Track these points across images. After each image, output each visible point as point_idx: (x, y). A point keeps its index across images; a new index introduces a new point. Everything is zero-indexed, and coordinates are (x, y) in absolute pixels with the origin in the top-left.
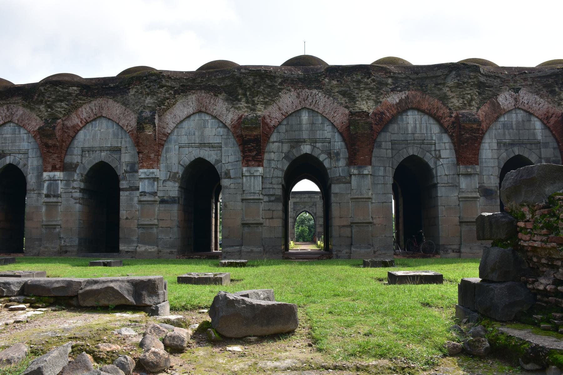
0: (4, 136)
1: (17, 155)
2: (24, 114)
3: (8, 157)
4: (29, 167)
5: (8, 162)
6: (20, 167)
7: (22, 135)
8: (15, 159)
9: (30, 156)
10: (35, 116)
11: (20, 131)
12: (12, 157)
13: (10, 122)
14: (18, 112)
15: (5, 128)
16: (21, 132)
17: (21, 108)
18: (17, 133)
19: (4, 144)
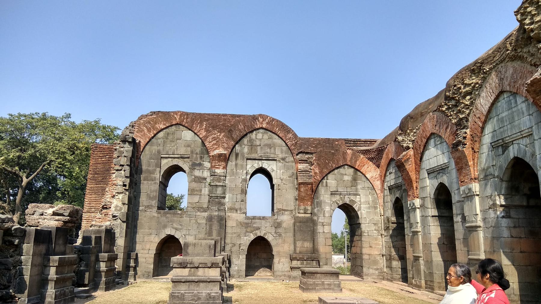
0: (500, 117)
1: (521, 141)
2: (515, 71)
3: (511, 148)
4: (538, 156)
5: (512, 156)
6: (527, 159)
7: (519, 107)
8: (519, 149)
9: (536, 138)
10: (529, 67)
11: (516, 101)
12: (516, 146)
13: (501, 92)
14: (508, 72)
15: (499, 104)
16: (519, 102)
17: (509, 64)
18: (513, 105)
19: (502, 130)
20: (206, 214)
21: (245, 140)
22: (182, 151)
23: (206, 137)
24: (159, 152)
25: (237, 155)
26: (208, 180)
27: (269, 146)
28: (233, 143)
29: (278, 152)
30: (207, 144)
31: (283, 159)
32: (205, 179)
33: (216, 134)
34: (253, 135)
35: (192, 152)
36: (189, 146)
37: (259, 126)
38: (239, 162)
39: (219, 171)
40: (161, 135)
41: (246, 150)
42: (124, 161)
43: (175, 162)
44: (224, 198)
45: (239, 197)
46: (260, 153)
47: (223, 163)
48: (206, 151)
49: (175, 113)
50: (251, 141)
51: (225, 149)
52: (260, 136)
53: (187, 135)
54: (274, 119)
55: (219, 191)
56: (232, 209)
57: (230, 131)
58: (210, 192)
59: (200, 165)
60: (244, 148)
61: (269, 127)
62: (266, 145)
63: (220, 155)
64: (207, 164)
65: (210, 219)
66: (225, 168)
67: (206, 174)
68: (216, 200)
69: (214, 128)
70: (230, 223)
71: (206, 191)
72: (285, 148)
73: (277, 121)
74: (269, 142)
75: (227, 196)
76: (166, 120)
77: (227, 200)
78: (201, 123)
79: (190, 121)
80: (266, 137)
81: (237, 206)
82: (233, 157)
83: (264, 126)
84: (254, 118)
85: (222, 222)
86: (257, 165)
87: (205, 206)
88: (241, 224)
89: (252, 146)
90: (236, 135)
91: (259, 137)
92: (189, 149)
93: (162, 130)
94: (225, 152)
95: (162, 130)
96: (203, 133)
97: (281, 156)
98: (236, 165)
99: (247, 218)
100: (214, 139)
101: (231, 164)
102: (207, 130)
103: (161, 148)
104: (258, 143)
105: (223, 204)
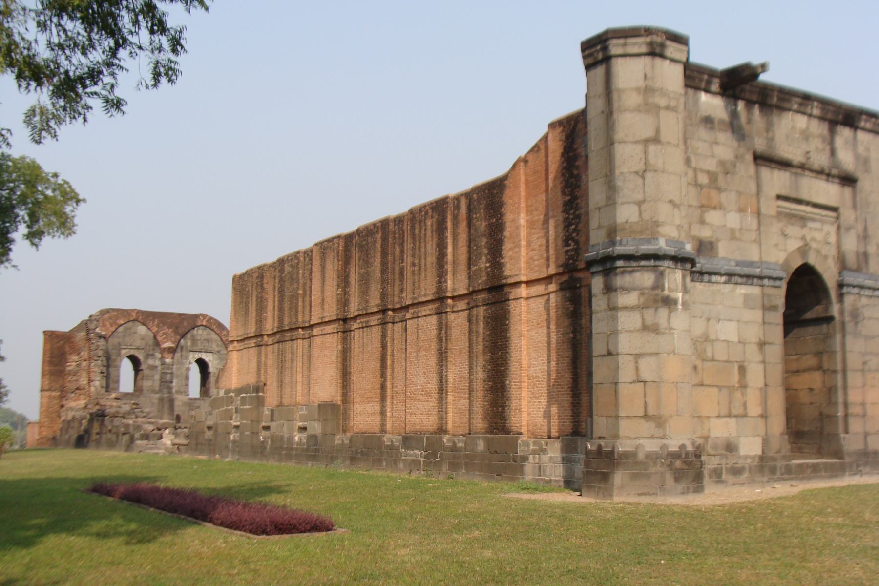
20: (157, 396)
21: (189, 335)
22: (138, 343)
23: (158, 332)
24: (119, 344)
25: (182, 348)
26: (159, 368)
27: (208, 341)
28: (179, 337)
29: (214, 346)
30: (159, 338)
31: (219, 352)
32: (156, 367)
33: (166, 329)
34: (195, 331)
35: (146, 344)
36: (143, 339)
37: (199, 323)
38: (184, 353)
39: (168, 361)
40: (121, 329)
41: (189, 343)
42: (100, 353)
43: (132, 352)
44: (172, 382)
45: (184, 382)
46: (200, 346)
47: (171, 355)
48: (157, 344)
49: (133, 310)
50: (193, 337)
51: (173, 343)
52: (200, 332)
53: (142, 329)
54: (212, 318)
55: (168, 377)
56: (177, 392)
57: (177, 328)
58: (161, 378)
59: (153, 355)
60: (187, 342)
61: (208, 324)
62: (206, 340)
63: (170, 348)
64: (158, 355)
65: (161, 400)
66: (173, 358)
67: (158, 363)
68: (166, 383)
69: (164, 324)
70: (177, 403)
71: (157, 377)
72: (220, 343)
73: (216, 320)
74: (207, 337)
75: (175, 381)
76: (125, 317)
77: (174, 384)
78: (153, 320)
79: (146, 317)
80: (205, 333)
81: (182, 389)
82: (179, 349)
83: (204, 323)
84: (196, 317)
85: (171, 402)
86: (197, 356)
87: (157, 389)
88: (185, 404)
89: (194, 341)
90: (181, 331)
91: (199, 332)
92: (143, 342)
93: (121, 325)
94: (173, 345)
95: (121, 325)
96: (155, 329)
97: (217, 349)
98: (181, 356)
99: (191, 399)
100: (164, 334)
101: (178, 355)
102: (158, 326)
103: (121, 340)
104: (199, 338)
105: (171, 388)
